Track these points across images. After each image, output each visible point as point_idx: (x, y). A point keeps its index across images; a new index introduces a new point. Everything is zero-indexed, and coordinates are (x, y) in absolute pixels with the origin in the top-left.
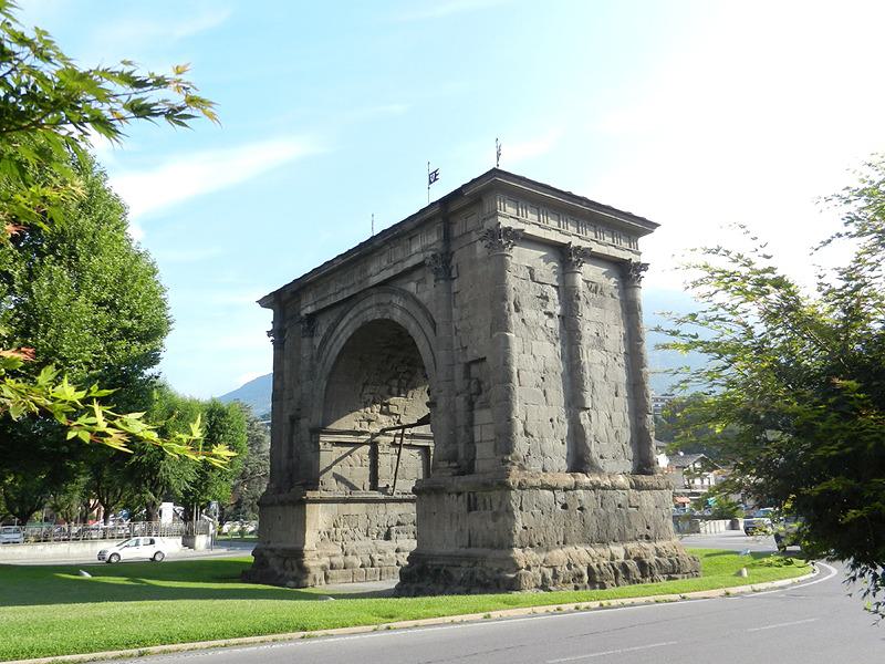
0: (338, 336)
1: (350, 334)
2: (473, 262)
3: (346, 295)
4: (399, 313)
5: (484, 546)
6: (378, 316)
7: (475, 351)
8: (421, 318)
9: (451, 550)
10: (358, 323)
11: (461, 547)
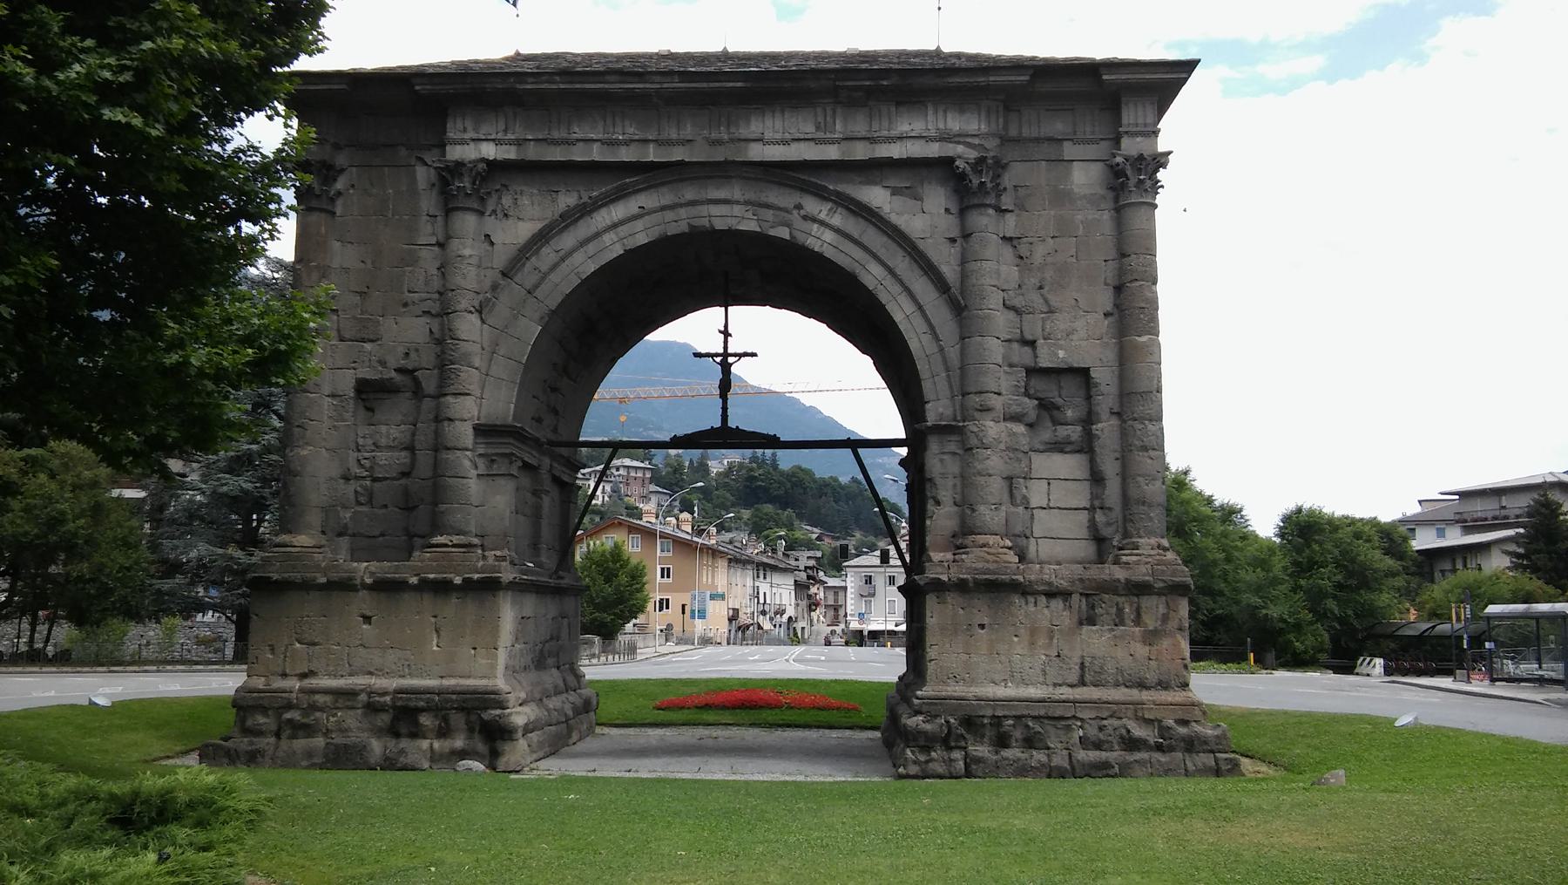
0: (597, 235)
1: (642, 239)
2: (1061, 197)
3: (652, 155)
4: (828, 236)
5: (1117, 685)
6: (750, 225)
7: (1061, 354)
8: (902, 263)
9: (1034, 692)
10: (677, 222)
11: (1055, 685)
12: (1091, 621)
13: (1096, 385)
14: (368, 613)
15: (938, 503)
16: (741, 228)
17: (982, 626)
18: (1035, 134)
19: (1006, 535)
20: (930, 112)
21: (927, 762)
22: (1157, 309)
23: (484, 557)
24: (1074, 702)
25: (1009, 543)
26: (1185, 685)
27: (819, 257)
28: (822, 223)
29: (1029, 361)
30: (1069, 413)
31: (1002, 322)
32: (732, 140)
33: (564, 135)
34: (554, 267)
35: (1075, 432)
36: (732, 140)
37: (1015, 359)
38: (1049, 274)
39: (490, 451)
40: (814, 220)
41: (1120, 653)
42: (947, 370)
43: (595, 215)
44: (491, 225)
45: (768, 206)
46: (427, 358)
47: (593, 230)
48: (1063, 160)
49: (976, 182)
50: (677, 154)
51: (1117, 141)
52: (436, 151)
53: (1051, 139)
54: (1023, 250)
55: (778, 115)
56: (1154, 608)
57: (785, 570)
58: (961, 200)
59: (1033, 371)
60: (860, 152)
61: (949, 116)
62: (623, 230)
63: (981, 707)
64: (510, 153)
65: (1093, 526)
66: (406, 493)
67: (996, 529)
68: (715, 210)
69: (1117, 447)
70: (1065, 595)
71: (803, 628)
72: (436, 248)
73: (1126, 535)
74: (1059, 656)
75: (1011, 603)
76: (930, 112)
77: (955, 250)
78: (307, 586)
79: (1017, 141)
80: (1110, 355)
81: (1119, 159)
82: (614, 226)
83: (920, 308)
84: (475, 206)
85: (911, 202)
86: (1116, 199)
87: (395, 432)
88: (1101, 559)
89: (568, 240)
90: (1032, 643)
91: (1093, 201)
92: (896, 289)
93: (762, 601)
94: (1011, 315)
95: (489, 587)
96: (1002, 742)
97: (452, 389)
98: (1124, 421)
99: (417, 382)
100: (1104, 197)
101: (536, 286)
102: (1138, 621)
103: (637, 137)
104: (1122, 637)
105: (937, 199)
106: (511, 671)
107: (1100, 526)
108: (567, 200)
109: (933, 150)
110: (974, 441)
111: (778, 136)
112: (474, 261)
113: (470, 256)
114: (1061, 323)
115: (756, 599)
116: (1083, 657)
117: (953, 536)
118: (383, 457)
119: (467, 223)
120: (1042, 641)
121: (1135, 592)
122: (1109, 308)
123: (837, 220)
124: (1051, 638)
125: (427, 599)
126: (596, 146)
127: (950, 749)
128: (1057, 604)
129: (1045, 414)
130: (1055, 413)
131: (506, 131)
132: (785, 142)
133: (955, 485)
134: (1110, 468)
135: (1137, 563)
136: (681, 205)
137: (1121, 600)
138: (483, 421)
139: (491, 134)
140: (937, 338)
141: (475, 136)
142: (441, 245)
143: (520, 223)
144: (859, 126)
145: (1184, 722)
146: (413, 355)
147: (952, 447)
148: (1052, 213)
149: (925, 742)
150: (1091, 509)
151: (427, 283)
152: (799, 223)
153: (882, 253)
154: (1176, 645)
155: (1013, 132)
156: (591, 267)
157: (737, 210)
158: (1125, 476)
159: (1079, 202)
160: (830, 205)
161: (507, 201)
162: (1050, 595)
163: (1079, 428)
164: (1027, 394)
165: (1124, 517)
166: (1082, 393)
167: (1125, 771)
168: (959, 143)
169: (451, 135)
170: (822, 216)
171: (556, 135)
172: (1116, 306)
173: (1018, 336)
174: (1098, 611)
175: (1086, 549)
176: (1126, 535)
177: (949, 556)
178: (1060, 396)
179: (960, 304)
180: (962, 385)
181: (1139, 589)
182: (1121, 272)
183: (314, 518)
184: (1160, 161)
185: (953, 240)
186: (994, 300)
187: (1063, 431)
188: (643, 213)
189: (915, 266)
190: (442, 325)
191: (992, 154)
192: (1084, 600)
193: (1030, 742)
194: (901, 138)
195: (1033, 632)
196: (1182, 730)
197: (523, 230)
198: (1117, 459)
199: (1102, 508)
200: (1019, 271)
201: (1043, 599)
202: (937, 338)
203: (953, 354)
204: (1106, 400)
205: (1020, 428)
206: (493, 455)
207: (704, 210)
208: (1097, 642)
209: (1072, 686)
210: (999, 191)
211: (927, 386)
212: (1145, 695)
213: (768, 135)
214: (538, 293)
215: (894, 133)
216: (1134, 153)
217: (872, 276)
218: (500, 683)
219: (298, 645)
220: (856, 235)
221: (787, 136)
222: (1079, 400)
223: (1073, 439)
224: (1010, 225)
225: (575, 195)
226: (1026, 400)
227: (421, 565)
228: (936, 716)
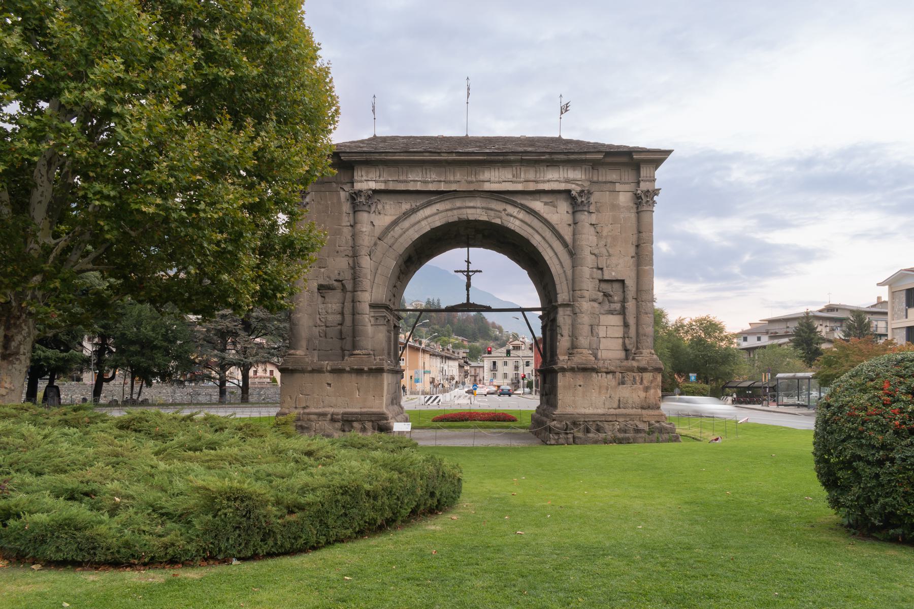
0: (419, 222)
1: (438, 224)
2: (614, 207)
3: (443, 187)
4: (517, 223)
5: (632, 408)
6: (484, 218)
7: (613, 274)
8: (548, 234)
9: (600, 411)
10: (453, 217)
11: (609, 409)
12: (623, 383)
13: (627, 287)
14: (329, 382)
15: (562, 336)
16: (480, 219)
17: (580, 386)
18: (604, 180)
19: (589, 349)
20: (561, 170)
22: (653, 255)
23: (375, 359)
24: (616, 415)
25: (591, 352)
26: (659, 408)
27: (513, 232)
28: (515, 217)
29: (600, 277)
30: (616, 298)
31: (589, 260)
32: (477, 181)
33: (405, 178)
34: (401, 236)
35: (618, 306)
36: (477, 181)
37: (595, 276)
38: (609, 240)
39: (376, 315)
40: (511, 216)
41: (635, 396)
42: (567, 280)
43: (418, 213)
44: (373, 217)
45: (491, 209)
46: (347, 275)
47: (417, 219)
49: (579, 200)
50: (453, 187)
51: (638, 183)
52: (349, 185)
54: (598, 229)
55: (497, 170)
56: (648, 376)
58: (573, 208)
59: (602, 281)
60: (532, 187)
61: (569, 172)
62: (429, 220)
63: (579, 418)
64: (382, 186)
65: (624, 344)
66: (341, 332)
67: (586, 346)
68: (469, 211)
69: (635, 312)
70: (613, 372)
72: (350, 228)
73: (637, 348)
75: (592, 377)
76: (561, 170)
77: (571, 229)
78: (303, 371)
79: (597, 182)
80: (633, 274)
81: (639, 192)
82: (426, 218)
83: (556, 254)
84: (367, 209)
85: (552, 208)
86: (637, 208)
87: (334, 307)
88: (627, 358)
89: (406, 224)
90: (600, 392)
92: (546, 246)
94: (593, 257)
95: (380, 371)
96: (588, 431)
97: (360, 289)
98: (638, 302)
99: (343, 285)
101: (393, 244)
102: (641, 383)
104: (635, 389)
105: (564, 206)
106: (387, 406)
107: (627, 345)
108: (406, 206)
109: (563, 186)
110: (577, 310)
111: (497, 179)
112: (367, 233)
114: (614, 261)
118: (330, 318)
119: (364, 217)
120: (604, 391)
122: (633, 254)
123: (522, 215)
124: (607, 390)
125: (354, 376)
126: (419, 183)
128: (610, 376)
129: (606, 299)
131: (380, 176)
132: (499, 182)
134: (632, 321)
135: (642, 360)
136: (455, 209)
137: (634, 374)
138: (372, 302)
140: (562, 267)
141: (367, 179)
142: (351, 226)
143: (386, 217)
144: (531, 175)
145: (658, 422)
146: (342, 274)
147: (568, 313)
150: (624, 338)
151: (347, 243)
152: (505, 217)
153: (540, 231)
154: (656, 392)
155: (595, 179)
156: (417, 236)
157: (478, 211)
158: (638, 324)
160: (518, 209)
161: (380, 207)
162: (607, 373)
163: (619, 305)
164: (599, 291)
166: (621, 290)
167: (635, 441)
169: (356, 178)
170: (515, 214)
171: (401, 178)
172: (636, 253)
173: (596, 266)
174: (626, 379)
175: (622, 354)
176: (637, 348)
179: (573, 252)
181: (642, 370)
182: (639, 239)
183: (304, 343)
184: (656, 192)
186: (586, 252)
187: (613, 306)
188: (439, 212)
189: (554, 237)
190: (354, 261)
191: (587, 189)
193: (599, 430)
194: (549, 181)
195: (600, 387)
196: (657, 425)
197: (387, 220)
201: (604, 374)
202: (562, 267)
203: (569, 273)
205: (596, 305)
207: (464, 211)
208: (625, 392)
209: (615, 409)
210: (589, 203)
211: (558, 287)
212: (644, 412)
213: (492, 179)
214: (394, 247)
215: (546, 179)
216: (645, 189)
217: (536, 240)
218: (385, 410)
220: (529, 222)
221: (501, 180)
222: (620, 293)
224: (593, 219)
225: (409, 204)
226: (599, 293)
227: (349, 362)
228: (561, 421)
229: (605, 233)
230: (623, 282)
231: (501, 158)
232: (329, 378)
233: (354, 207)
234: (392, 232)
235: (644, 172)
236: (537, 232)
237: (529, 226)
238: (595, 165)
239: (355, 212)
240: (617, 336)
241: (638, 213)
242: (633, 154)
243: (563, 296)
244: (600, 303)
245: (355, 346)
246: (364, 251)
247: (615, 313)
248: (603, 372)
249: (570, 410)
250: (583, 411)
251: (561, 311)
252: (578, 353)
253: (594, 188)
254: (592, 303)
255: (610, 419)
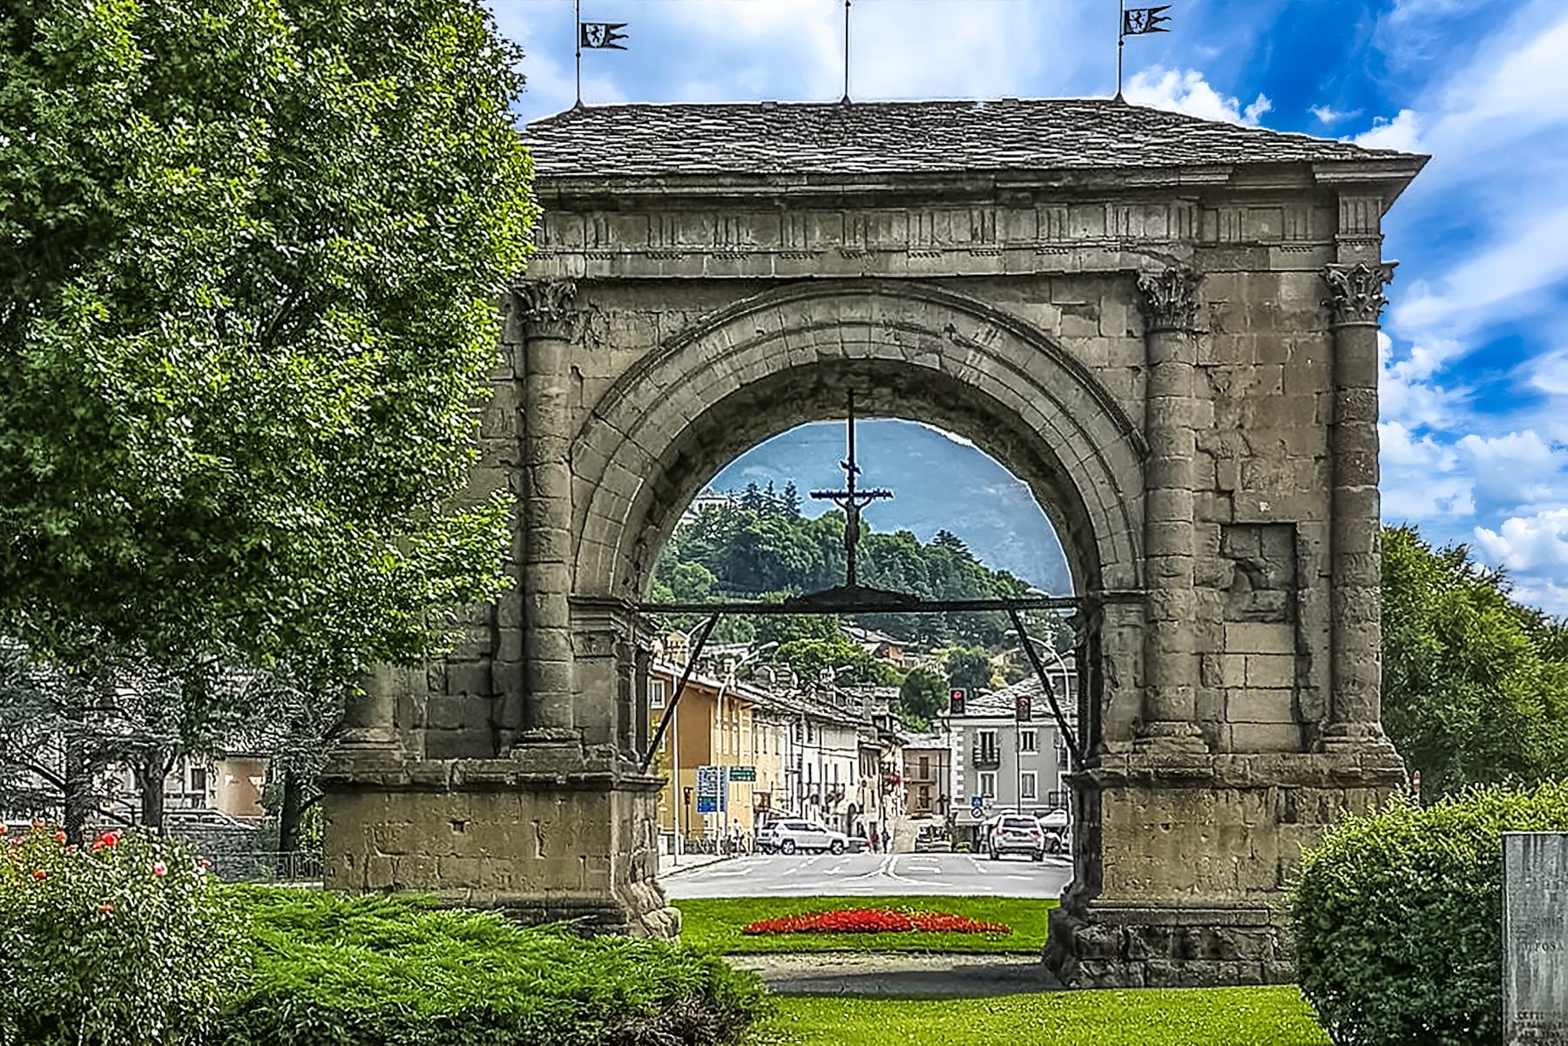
0: (708, 365)
1: (762, 372)
2: (1265, 316)
3: (774, 268)
4: (987, 365)
7: (1263, 506)
8: (1073, 396)
10: (806, 350)
12: (1291, 818)
21: (1102, 976)
28: (979, 349)
29: (1225, 517)
30: (1272, 575)
34: (656, 405)
35: (1278, 598)
36: (870, 252)
39: (587, 629)
42: (1128, 526)
48: (1269, 271)
50: (806, 267)
51: (1334, 246)
53: (1254, 245)
57: (842, 727)
58: (1146, 322)
60: (1026, 264)
65: (1296, 708)
66: (489, 674)
67: (1182, 715)
68: (849, 334)
70: (1262, 788)
71: (873, 824)
73: (1334, 719)
74: (1253, 858)
78: (388, 788)
79: (1216, 245)
80: (1320, 508)
83: (1097, 452)
86: (1332, 318)
88: (1305, 749)
89: (672, 372)
90: (1223, 845)
91: (1306, 321)
93: (805, 779)
96: (1185, 952)
100: (1317, 316)
101: (634, 429)
103: (755, 249)
105: (1118, 318)
107: (1304, 708)
108: (671, 323)
109: (1115, 261)
110: (1158, 612)
112: (561, 401)
113: (558, 395)
114: (1265, 469)
115: (796, 776)
116: (1279, 859)
117: (1134, 723)
121: (1342, 785)
122: (1321, 450)
125: (526, 801)
127: (1127, 960)
128: (1253, 799)
130: (1255, 574)
131: (597, 241)
133: (1136, 663)
134: (1317, 641)
135: (1342, 751)
136: (808, 329)
139: (578, 246)
144: (1024, 229)
147: (1133, 618)
148: (1255, 335)
149: (1102, 955)
150: (1296, 689)
151: (504, 428)
155: (1210, 237)
158: (1334, 649)
159: (1287, 322)
161: (597, 325)
162: (1244, 790)
164: (1222, 554)
165: (1332, 697)
166: (1289, 552)
168: (1143, 253)
170: (979, 340)
176: (1334, 719)
177: (1129, 745)
178: (1261, 556)
180: (1145, 550)
181: (1346, 780)
182: (1336, 407)
183: (387, 708)
185: (1136, 369)
187: (1264, 598)
188: (764, 337)
190: (525, 478)
191: (1183, 266)
192: (1282, 794)
193: (1217, 951)
195: (1224, 831)
197: (620, 360)
198: (1325, 631)
199: (1306, 688)
200: (1215, 406)
203: (1135, 506)
204: (1313, 569)
205: (1214, 596)
206: (591, 632)
217: (1040, 414)
219: (380, 855)
222: (1284, 561)
223: (1275, 607)
227: (509, 764)
228: (1113, 927)
229: (1238, 392)
230: (1290, 530)
231: (939, 187)
232: (459, 805)
233: (524, 329)
234: (631, 396)
235: (1350, 215)
236: (1042, 389)
237: (1020, 373)
238: (1207, 199)
239: (527, 342)
240: (1276, 682)
241: (1333, 331)
242: (1315, 168)
243: (1118, 570)
244: (1226, 590)
245: (529, 714)
246: (553, 451)
247: (1274, 615)
248: (1231, 787)
249: (1134, 896)
250: (1174, 896)
251: (1111, 614)
252: (1159, 733)
253: (1209, 262)
254: (1203, 591)
255: (1252, 921)
